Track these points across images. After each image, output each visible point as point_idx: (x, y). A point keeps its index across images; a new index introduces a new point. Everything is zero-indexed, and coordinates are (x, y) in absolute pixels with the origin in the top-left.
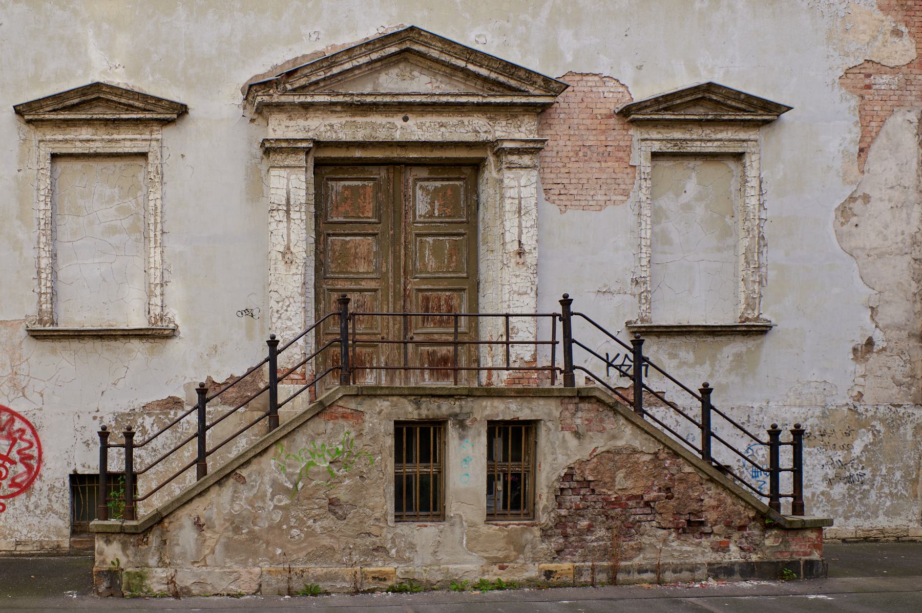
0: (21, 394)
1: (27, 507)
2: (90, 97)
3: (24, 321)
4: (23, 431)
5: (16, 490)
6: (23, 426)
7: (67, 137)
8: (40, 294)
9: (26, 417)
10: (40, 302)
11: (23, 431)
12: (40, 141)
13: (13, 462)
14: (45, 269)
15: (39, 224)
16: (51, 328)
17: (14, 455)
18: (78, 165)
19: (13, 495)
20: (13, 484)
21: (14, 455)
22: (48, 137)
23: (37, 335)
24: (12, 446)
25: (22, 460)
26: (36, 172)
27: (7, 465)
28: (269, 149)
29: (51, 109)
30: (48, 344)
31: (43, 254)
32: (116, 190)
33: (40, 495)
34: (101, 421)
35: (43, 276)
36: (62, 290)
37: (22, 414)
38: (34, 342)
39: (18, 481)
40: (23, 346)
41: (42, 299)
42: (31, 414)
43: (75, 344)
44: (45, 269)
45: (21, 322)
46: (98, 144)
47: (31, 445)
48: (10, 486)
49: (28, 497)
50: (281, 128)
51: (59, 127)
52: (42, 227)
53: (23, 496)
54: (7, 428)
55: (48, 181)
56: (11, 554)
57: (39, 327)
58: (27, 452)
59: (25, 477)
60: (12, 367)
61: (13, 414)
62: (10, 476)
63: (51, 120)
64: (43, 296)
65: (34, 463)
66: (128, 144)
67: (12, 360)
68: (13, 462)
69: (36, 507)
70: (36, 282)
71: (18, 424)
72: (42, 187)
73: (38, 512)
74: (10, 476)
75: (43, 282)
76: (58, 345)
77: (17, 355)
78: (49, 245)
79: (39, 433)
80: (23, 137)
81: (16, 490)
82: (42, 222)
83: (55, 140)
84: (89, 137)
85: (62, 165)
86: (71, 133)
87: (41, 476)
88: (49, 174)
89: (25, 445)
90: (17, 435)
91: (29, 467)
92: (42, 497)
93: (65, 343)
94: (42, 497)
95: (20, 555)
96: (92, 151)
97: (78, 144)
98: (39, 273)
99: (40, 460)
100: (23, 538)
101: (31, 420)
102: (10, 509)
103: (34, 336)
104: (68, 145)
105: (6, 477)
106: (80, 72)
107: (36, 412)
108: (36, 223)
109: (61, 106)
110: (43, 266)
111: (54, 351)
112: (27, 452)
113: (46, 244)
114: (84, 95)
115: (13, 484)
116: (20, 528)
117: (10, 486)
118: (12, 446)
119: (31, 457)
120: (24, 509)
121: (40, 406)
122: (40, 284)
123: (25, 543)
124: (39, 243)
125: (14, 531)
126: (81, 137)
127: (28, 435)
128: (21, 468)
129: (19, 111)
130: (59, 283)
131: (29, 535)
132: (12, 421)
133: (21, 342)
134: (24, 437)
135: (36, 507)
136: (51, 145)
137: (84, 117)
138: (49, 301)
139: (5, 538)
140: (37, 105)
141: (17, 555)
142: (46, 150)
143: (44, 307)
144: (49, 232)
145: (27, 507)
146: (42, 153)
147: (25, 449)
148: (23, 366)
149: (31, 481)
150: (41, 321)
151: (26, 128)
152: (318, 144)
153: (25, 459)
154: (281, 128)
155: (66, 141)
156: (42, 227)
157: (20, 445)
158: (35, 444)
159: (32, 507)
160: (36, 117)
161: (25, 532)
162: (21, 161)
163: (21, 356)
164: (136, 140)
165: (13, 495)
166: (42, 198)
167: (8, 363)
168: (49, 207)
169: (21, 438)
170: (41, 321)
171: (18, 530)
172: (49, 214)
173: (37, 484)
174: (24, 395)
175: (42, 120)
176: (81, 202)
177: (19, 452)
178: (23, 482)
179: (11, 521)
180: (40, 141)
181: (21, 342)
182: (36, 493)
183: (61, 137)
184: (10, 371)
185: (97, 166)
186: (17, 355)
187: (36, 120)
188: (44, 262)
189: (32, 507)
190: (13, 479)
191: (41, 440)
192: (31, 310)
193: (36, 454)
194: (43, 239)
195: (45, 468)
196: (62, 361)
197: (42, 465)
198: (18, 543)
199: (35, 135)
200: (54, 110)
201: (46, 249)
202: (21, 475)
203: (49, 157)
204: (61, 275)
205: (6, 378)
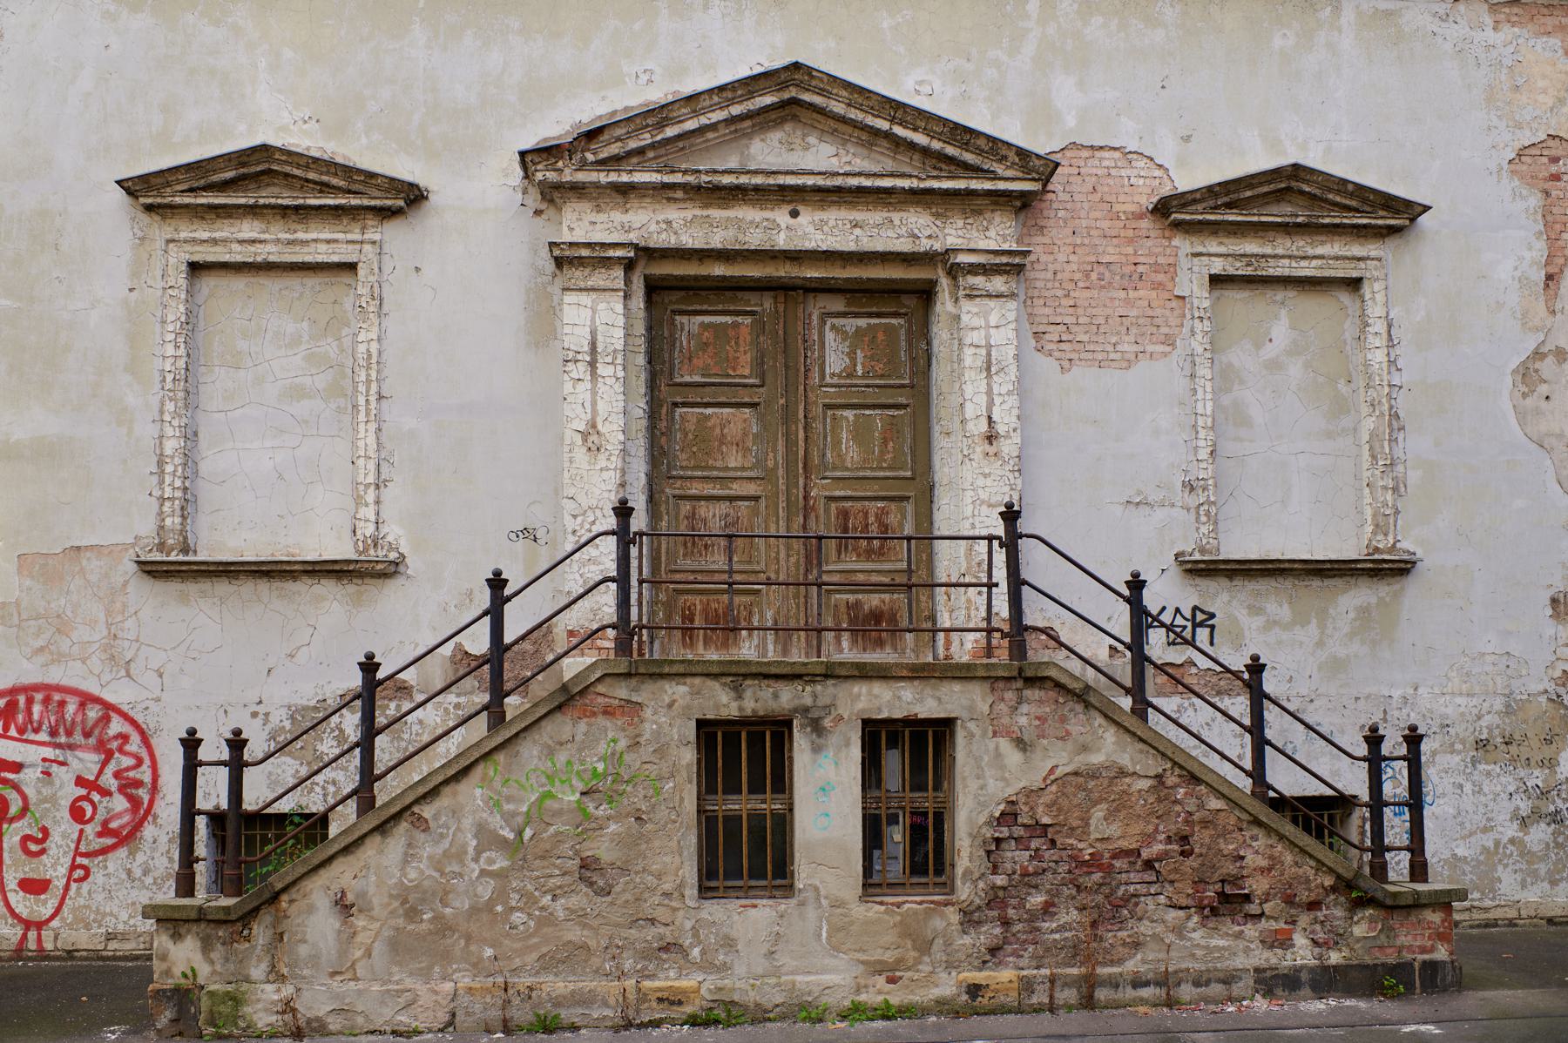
0: (123, 673)
1: (129, 872)
2: (253, 169)
3: (133, 545)
4: (125, 738)
5: (110, 841)
6: (127, 728)
7: (217, 235)
8: (162, 500)
9: (132, 714)
10: (160, 513)
11: (125, 738)
12: (169, 241)
13: (106, 793)
14: (172, 457)
15: (164, 380)
16: (181, 558)
17: (108, 780)
18: (239, 283)
19: (104, 851)
20: (105, 831)
21: (108, 780)
22: (183, 235)
23: (153, 571)
24: (104, 764)
25: (121, 790)
26: (159, 293)
27: (96, 797)
28: (565, 259)
29: (185, 186)
30: (174, 587)
31: (169, 431)
32: (305, 324)
33: (154, 850)
34: (266, 722)
35: (169, 468)
36: (207, 493)
37: (125, 708)
38: (148, 582)
39: (114, 825)
40: (130, 589)
41: (165, 509)
42: (140, 707)
43: (223, 587)
44: (172, 457)
45: (125, 547)
46: (270, 248)
47: (140, 762)
48: (100, 835)
49: (132, 854)
50: (583, 224)
51: (203, 218)
52: (169, 385)
53: (122, 852)
54: (96, 732)
55: (182, 309)
56: (96, 955)
57: (157, 557)
58: (131, 774)
59: (126, 818)
60: (109, 626)
61: (108, 707)
62: (100, 817)
63: (187, 206)
64: (167, 504)
65: (143, 794)
66: (323, 247)
67: (108, 613)
68: (106, 793)
69: (146, 872)
70: (155, 479)
71: (116, 726)
72: (171, 318)
73: (149, 880)
74: (100, 817)
75: (168, 479)
76: (192, 588)
77: (118, 605)
78: (180, 416)
79: (153, 742)
80: (140, 234)
81: (110, 841)
82: (169, 377)
83: (194, 241)
84: (254, 235)
85: (208, 283)
86: (224, 230)
87: (155, 817)
88: (183, 296)
89: (128, 762)
90: (114, 745)
91: (135, 802)
92: (156, 855)
93: (205, 585)
94: (156, 855)
95: (115, 958)
96: (259, 259)
97: (236, 247)
98: (161, 463)
99: (154, 788)
100: (121, 927)
101: (140, 719)
102: (97, 877)
103: (149, 573)
104: (218, 249)
105: (92, 819)
106: (242, 127)
107: (151, 704)
108: (158, 378)
109: (202, 182)
110: (168, 451)
111: (184, 599)
112: (131, 774)
113: (176, 414)
114: (243, 165)
115: (105, 831)
116: (115, 910)
117: (100, 835)
118: (104, 764)
119: (138, 784)
120: (124, 876)
121: (157, 693)
122: (161, 482)
123: (124, 937)
124: (162, 412)
125: (105, 915)
126: (241, 236)
127: (135, 745)
128: (120, 803)
129: (133, 187)
130: (200, 482)
131: (132, 922)
132: (106, 719)
133: (126, 583)
134: (127, 748)
135: (146, 872)
136: (187, 247)
137: (242, 201)
138: (178, 512)
139: (88, 927)
140: (159, 180)
141: (108, 958)
142: (179, 258)
143: (168, 522)
144: (181, 395)
145: (129, 872)
146: (172, 261)
147: (128, 769)
148: (129, 623)
149: (138, 826)
150: (161, 546)
151: (145, 218)
152: (649, 253)
153: (128, 786)
154: (583, 224)
155: (215, 242)
156: (169, 385)
157: (118, 762)
158: (147, 762)
159: (138, 873)
160: (159, 200)
161: (124, 916)
162: (135, 274)
163: (124, 606)
164: (335, 241)
165: (104, 851)
166: (171, 337)
167: (102, 616)
168: (182, 351)
169: (121, 750)
170: (161, 546)
171: (111, 914)
172: (181, 364)
173: (148, 831)
174: (128, 675)
175: (171, 207)
176: (242, 345)
177: (117, 775)
178: (123, 827)
179: (100, 897)
180: (169, 241)
181: (126, 583)
182: (146, 846)
183: (205, 235)
184: (105, 633)
185: (271, 285)
186: (118, 605)
187: (160, 206)
188: (170, 446)
189: (138, 873)
190: (105, 823)
191: (157, 753)
192: (146, 527)
193: (147, 778)
194: (170, 406)
195: (162, 804)
196: (200, 615)
197: (158, 797)
198: (110, 937)
199: (160, 231)
200: (191, 190)
201: (176, 423)
202: (119, 815)
203: (184, 267)
204: (204, 468)
205: (97, 645)
